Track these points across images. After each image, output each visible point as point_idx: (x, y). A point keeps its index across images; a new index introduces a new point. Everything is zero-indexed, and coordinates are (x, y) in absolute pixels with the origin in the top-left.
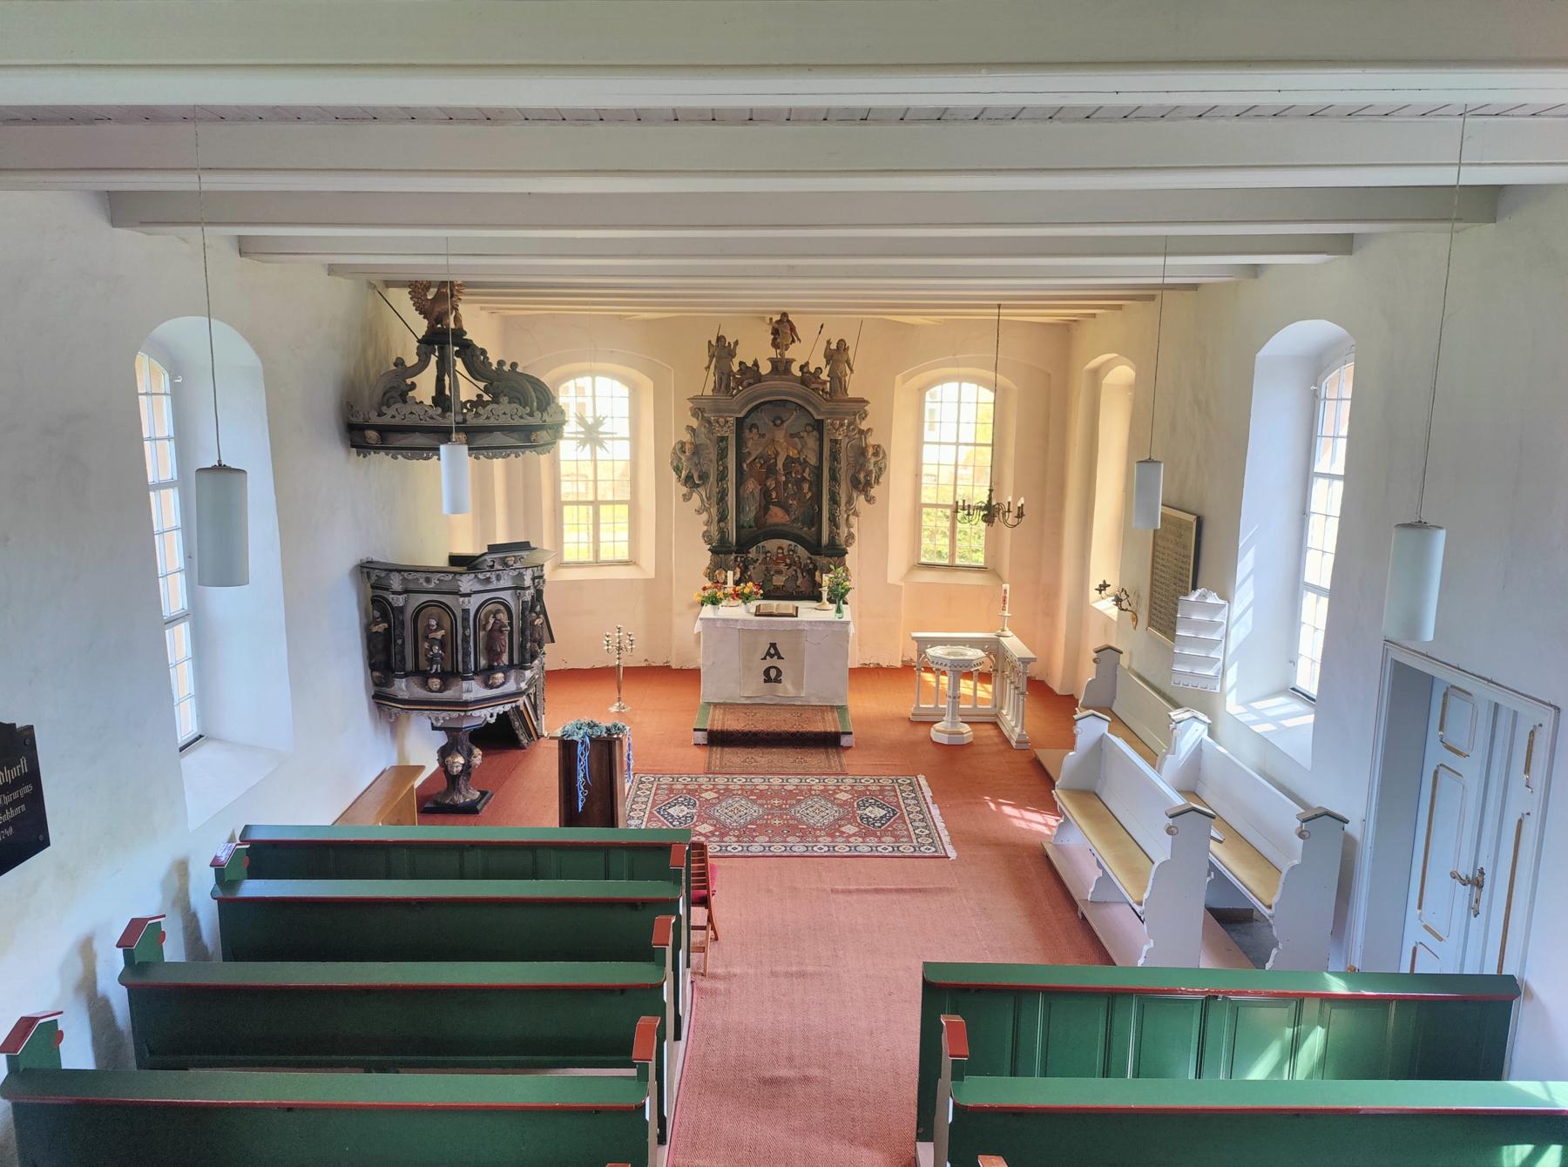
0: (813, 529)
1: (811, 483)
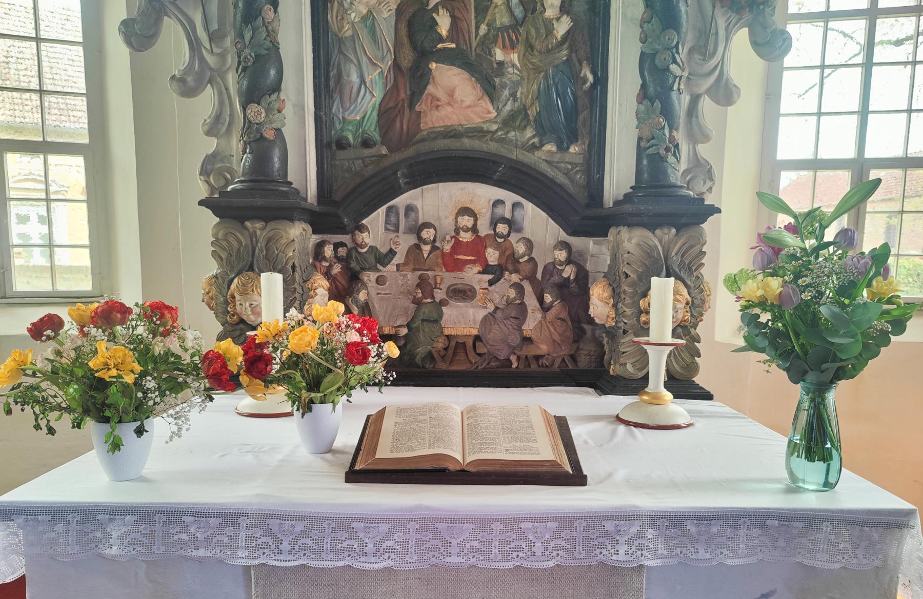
0: (574, 149)
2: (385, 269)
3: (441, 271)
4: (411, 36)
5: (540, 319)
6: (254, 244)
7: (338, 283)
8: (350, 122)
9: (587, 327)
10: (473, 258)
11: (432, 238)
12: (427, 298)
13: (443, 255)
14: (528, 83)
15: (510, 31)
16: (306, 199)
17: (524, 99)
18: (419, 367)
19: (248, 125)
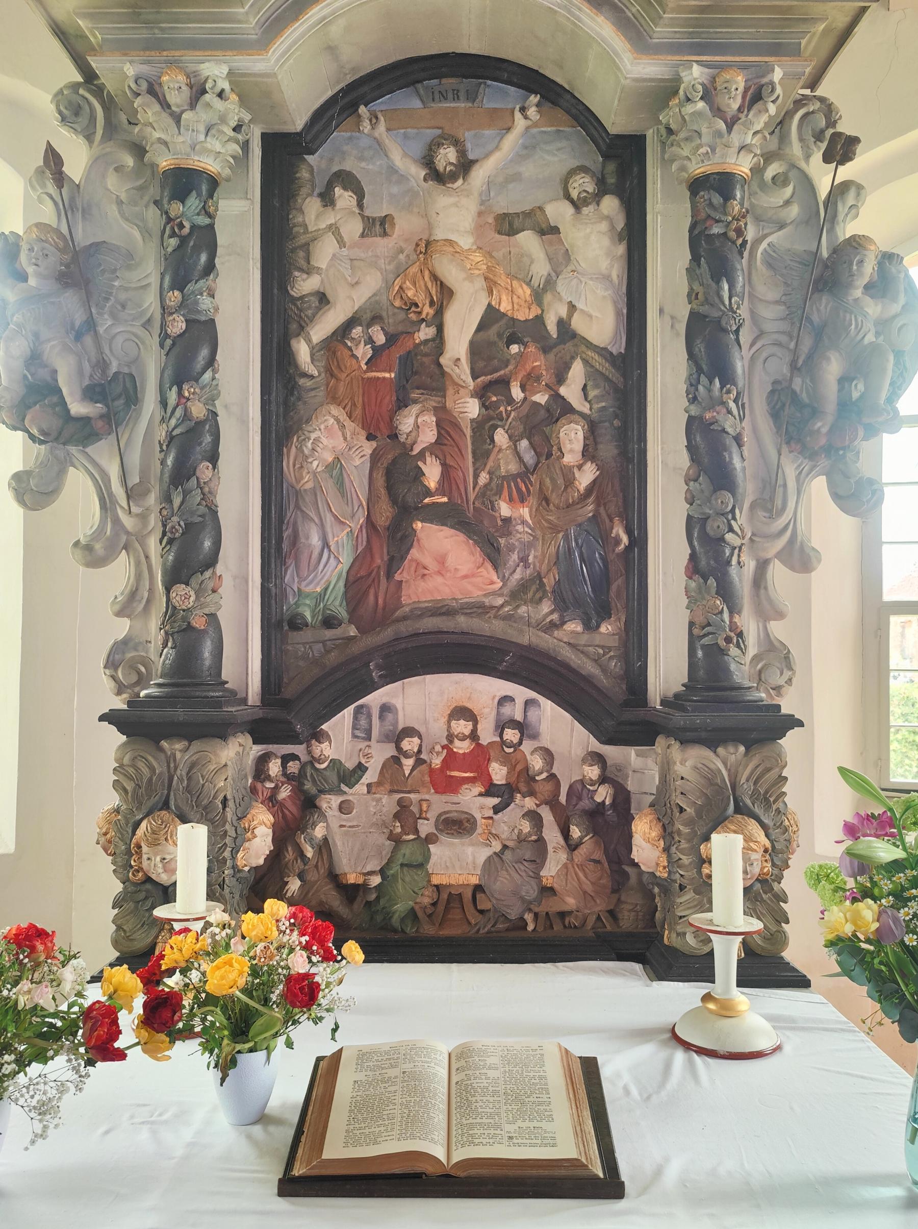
1: (592, 428)
2: (351, 791)
3: (428, 792)
4: (389, 488)
5: (565, 861)
6: (172, 770)
7: (287, 812)
8: (308, 595)
9: (628, 869)
10: (472, 775)
11: (416, 750)
12: (408, 834)
13: (432, 771)
14: (543, 544)
15: (519, 480)
16: (244, 701)
17: (538, 565)
18: (395, 931)
19: (172, 612)
